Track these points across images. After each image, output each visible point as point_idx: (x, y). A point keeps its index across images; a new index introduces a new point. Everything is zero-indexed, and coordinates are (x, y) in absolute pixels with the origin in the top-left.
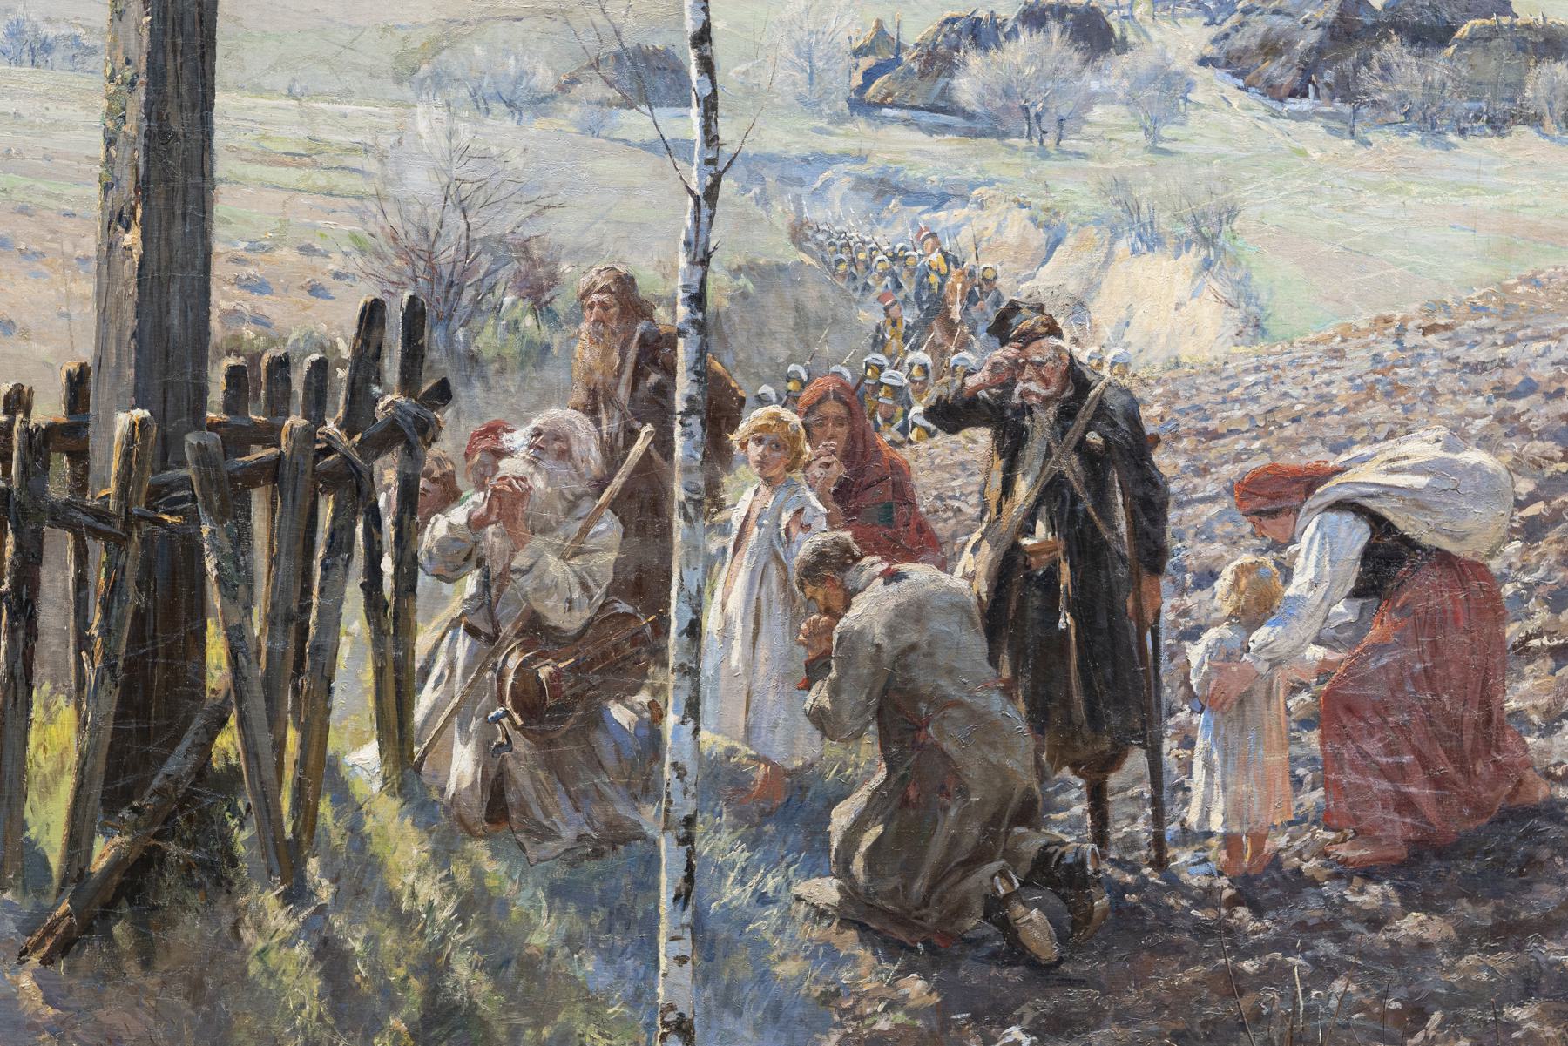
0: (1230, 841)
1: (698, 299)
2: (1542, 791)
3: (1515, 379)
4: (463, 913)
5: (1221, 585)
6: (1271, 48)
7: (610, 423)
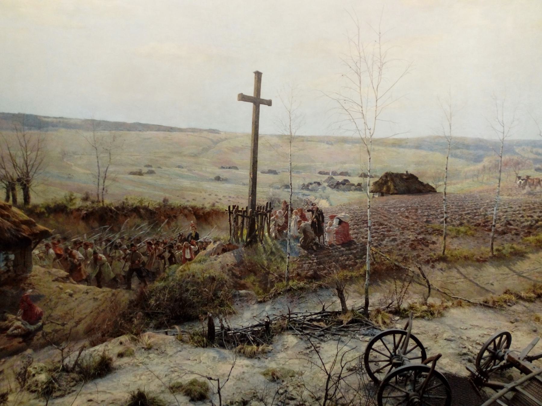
0: (329, 242)
1: (290, 202)
2: (352, 239)
4: (273, 245)
6: (332, 185)
7: (284, 211)
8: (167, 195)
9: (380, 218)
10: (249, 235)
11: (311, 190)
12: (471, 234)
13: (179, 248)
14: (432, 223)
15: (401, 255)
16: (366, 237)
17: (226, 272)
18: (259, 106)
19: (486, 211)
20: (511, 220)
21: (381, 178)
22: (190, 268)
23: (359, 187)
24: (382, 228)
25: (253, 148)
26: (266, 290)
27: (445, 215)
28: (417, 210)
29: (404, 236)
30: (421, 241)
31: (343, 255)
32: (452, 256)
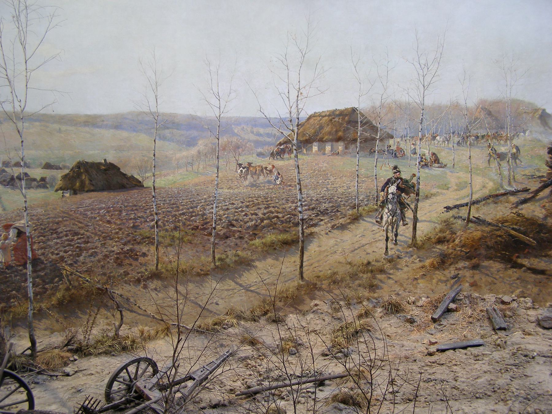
0: (5, 263)
2: (38, 257)
3: (32, 214)
5: (2, 236)
6: (4, 181)
9: (73, 224)
12: (188, 240)
14: (140, 229)
15: (104, 274)
16: (56, 252)
19: (205, 210)
20: (233, 220)
21: (72, 170)
23: (43, 183)
24: (77, 239)
27: (156, 218)
28: (120, 211)
29: (106, 248)
30: (128, 253)
32: (167, 270)
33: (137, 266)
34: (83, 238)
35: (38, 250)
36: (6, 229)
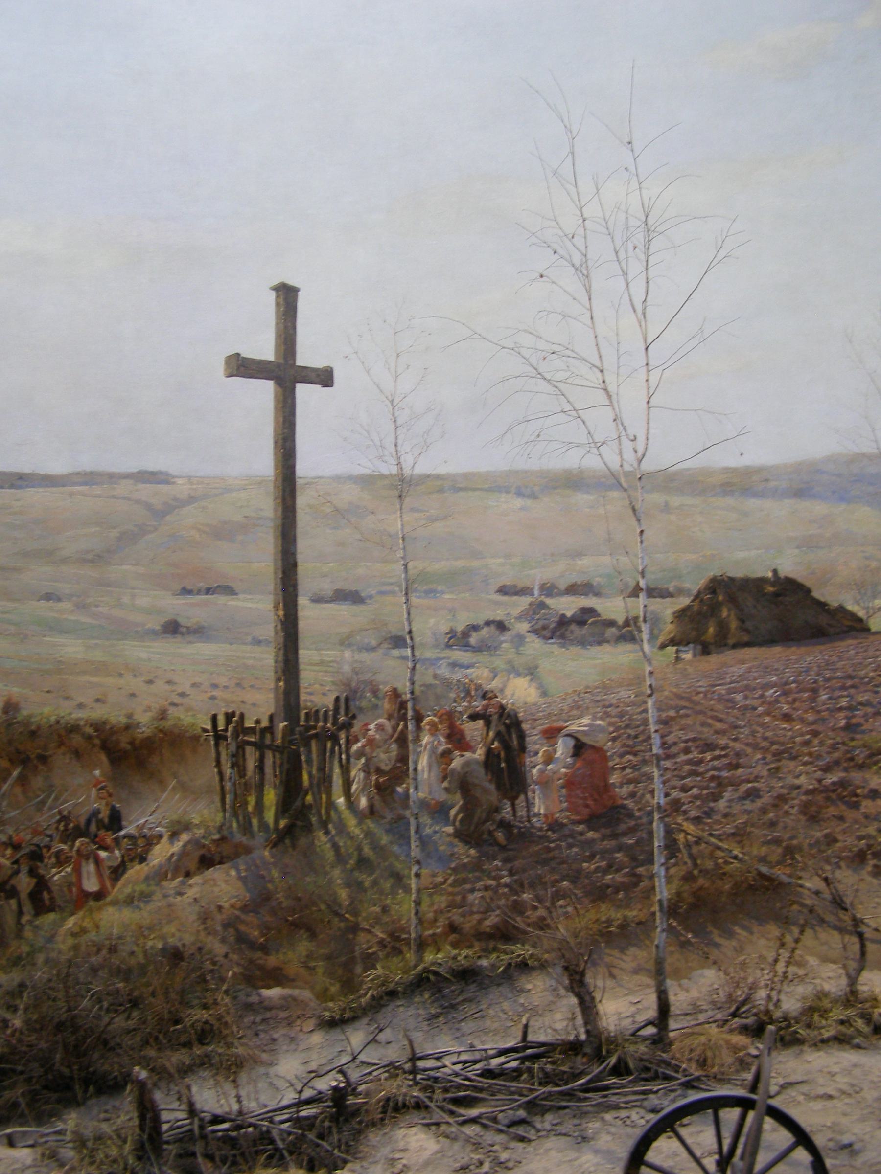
0: (546, 816)
1: (412, 693)
2: (620, 802)
3: (607, 703)
5: (540, 754)
6: (544, 628)
7: (393, 722)
8: (15, 691)
9: (703, 724)
10: (285, 806)
11: (477, 650)
13: (61, 860)
14: (863, 732)
17: (214, 933)
18: (294, 388)
21: (696, 597)
22: (102, 923)
24: (711, 760)
25: (279, 522)
26: (349, 985)
28: (815, 691)
29: (780, 779)
30: (834, 791)
31: (592, 856)
33: (856, 822)
34: (725, 756)
35: (621, 787)
36: (548, 738)
